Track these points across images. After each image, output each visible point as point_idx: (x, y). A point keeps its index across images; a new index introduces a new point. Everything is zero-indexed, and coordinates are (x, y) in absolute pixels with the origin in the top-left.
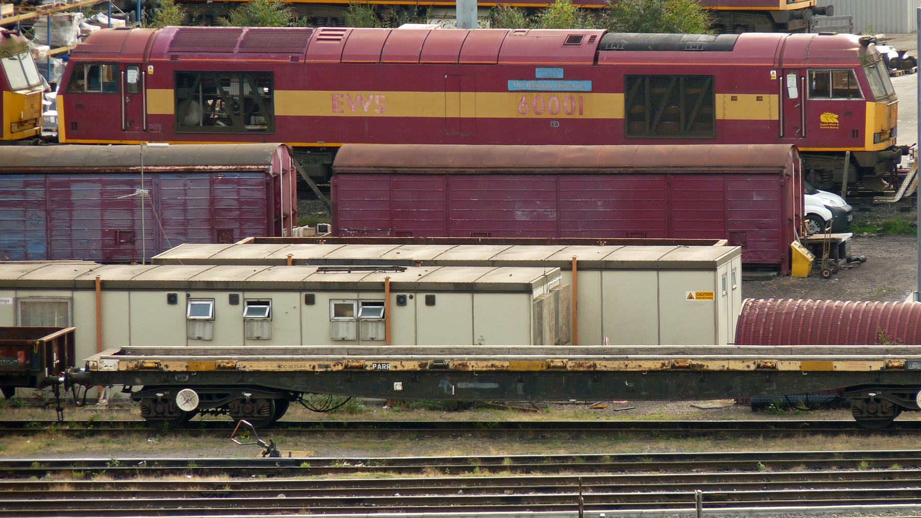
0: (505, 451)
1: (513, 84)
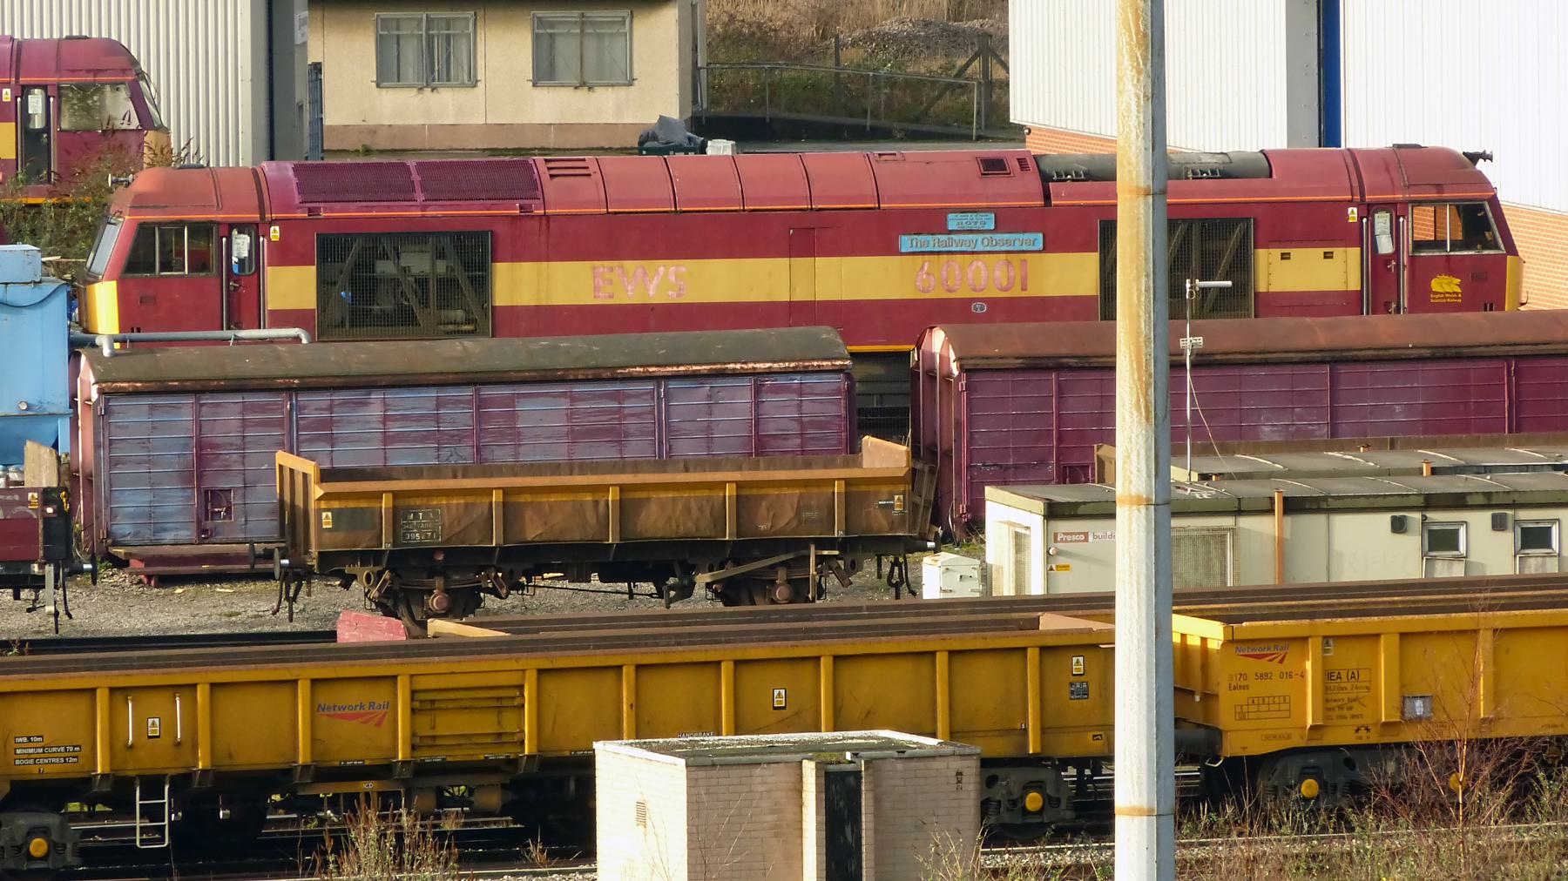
1: (906, 242)
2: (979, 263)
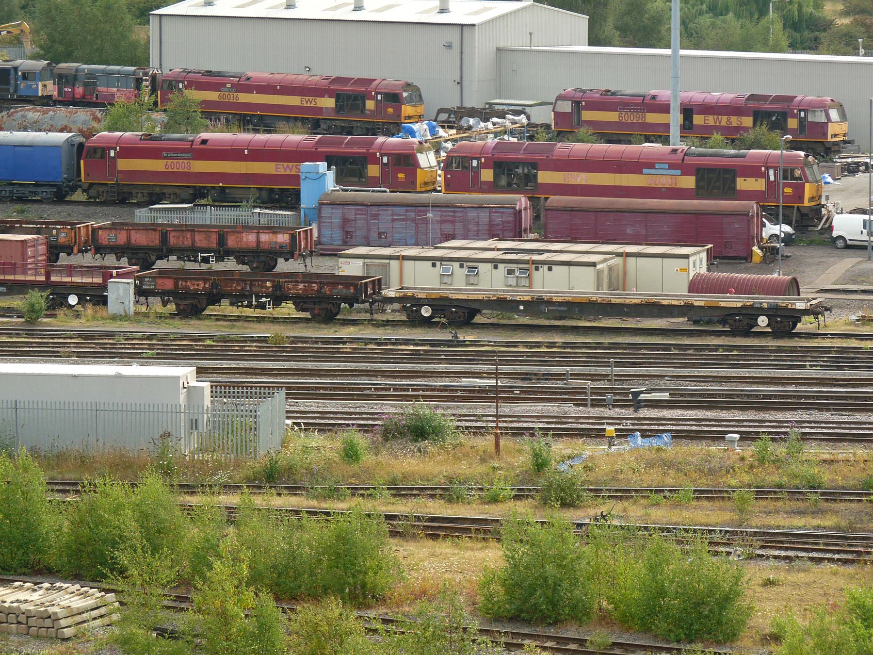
0: (558, 339)
1: (645, 171)
2: (664, 178)
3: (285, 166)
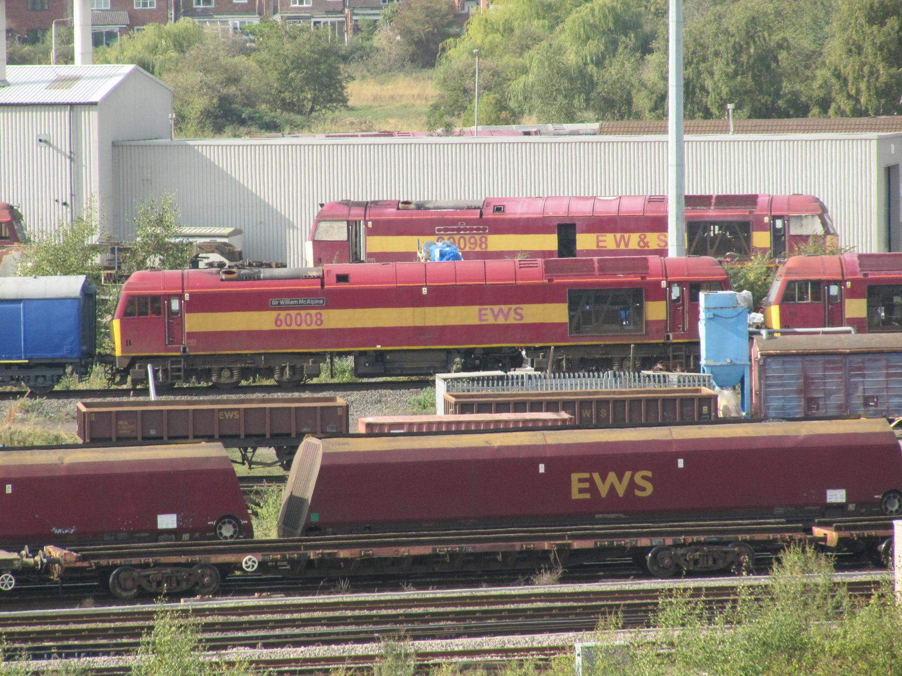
3: (496, 311)
